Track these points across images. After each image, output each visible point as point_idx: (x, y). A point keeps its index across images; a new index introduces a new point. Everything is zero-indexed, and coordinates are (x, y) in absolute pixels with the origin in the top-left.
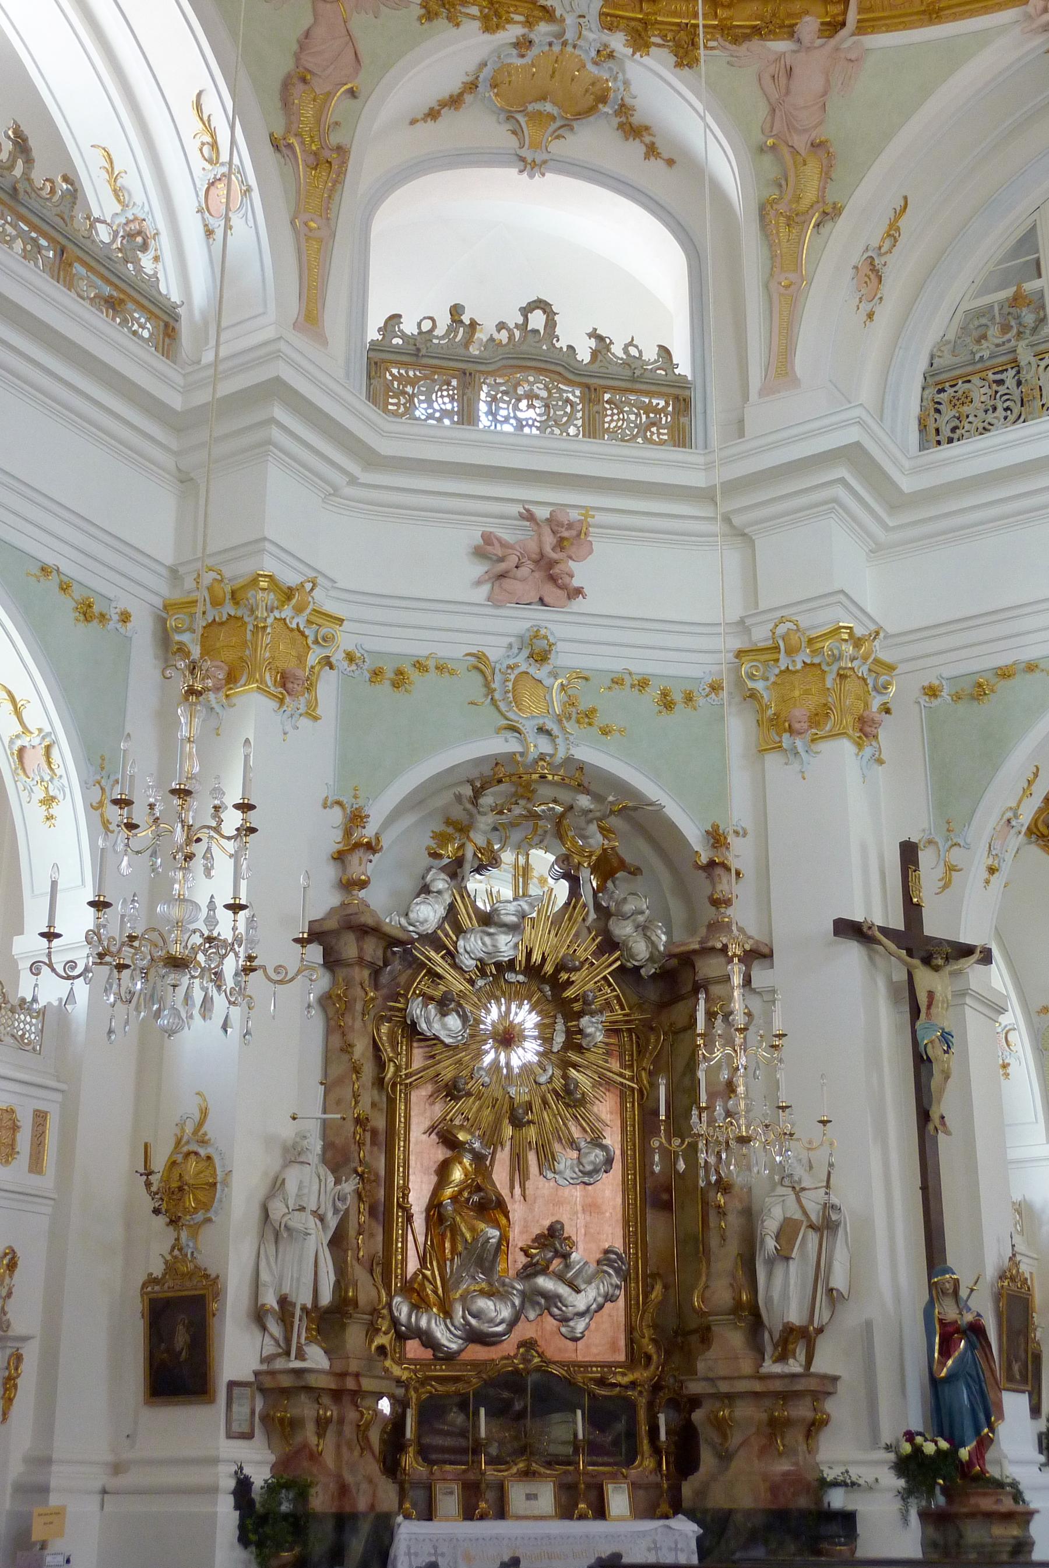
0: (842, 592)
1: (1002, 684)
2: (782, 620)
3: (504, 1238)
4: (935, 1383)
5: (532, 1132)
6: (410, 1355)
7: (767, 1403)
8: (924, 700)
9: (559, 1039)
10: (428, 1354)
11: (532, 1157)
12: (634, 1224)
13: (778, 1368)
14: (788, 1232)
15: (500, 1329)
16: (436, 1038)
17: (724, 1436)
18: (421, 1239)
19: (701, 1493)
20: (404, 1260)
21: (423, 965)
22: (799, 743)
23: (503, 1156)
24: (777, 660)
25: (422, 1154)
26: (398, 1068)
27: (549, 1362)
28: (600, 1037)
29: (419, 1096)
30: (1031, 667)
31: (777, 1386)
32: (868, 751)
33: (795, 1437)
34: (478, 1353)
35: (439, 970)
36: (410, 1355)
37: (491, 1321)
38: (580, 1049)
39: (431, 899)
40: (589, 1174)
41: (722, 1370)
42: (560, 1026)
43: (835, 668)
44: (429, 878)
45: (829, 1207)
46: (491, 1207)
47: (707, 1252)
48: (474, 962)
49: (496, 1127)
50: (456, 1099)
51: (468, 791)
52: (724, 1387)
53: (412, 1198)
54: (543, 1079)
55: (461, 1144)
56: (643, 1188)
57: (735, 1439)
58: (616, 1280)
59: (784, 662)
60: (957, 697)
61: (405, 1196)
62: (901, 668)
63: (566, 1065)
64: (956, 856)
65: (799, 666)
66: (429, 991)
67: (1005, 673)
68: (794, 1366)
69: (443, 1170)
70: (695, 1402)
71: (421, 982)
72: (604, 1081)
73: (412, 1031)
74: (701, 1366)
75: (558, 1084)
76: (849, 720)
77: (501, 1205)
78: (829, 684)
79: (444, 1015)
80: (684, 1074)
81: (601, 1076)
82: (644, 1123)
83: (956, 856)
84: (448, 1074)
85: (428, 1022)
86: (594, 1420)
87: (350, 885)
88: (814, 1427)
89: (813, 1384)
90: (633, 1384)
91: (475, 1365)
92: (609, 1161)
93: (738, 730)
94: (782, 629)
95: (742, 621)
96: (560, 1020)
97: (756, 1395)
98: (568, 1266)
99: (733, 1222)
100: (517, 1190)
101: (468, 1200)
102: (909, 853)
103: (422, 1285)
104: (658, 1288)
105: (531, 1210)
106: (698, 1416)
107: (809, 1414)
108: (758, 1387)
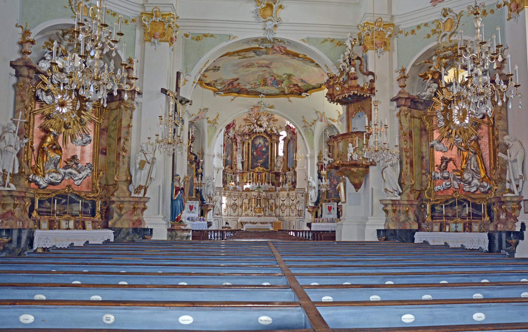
0: (172, 4)
1: (204, 38)
2: (156, 7)
3: (61, 158)
4: (172, 200)
5: (70, 131)
6: (32, 187)
7: (133, 203)
8: (184, 37)
9: (78, 107)
10: (37, 187)
11: (69, 137)
12: (94, 157)
13: (136, 195)
14: (142, 164)
15: (59, 181)
16: (44, 101)
17: (121, 211)
18: (36, 156)
19: (114, 224)
20: (31, 161)
21: (41, 80)
22: (156, 41)
23: (61, 136)
24: (152, 18)
25: (37, 132)
26: (32, 108)
27: (74, 191)
28: (91, 108)
29: (37, 117)
30: (212, 36)
31: (136, 200)
32: (172, 47)
33: (139, 211)
34: (52, 187)
35: (46, 83)
36: (32, 187)
37: (56, 179)
38: (85, 110)
39: (46, 61)
40: (85, 143)
41: (121, 195)
42: (79, 103)
43: (168, 24)
44: (45, 55)
45: (154, 158)
46: (58, 150)
47: (118, 166)
48: (57, 82)
49: (60, 128)
50: (49, 119)
51: (61, 32)
52: (122, 199)
53: (34, 145)
54: (73, 117)
55: (51, 132)
56: (99, 149)
57: (123, 212)
58: (89, 171)
59: (154, 19)
60: (193, 38)
61: (32, 144)
62: (180, 28)
63: (79, 114)
64: (187, 78)
65: (158, 21)
66: (42, 88)
67: (205, 36)
68: (141, 195)
69: (43, 139)
70: (113, 202)
71: (40, 85)
72: (91, 121)
73: (37, 99)
74: (115, 194)
75: (78, 119)
76: (169, 38)
77: (60, 149)
78: (166, 27)
79: (47, 95)
80: (113, 121)
81: (90, 118)
82: (102, 131)
83: (187, 78)
84: (47, 112)
85: (42, 97)
86: (85, 205)
87: (24, 53)
88: (144, 209)
89: (146, 200)
90: (94, 197)
91: (50, 190)
92: (90, 141)
93: (139, 33)
94: (155, 10)
95: (143, 5)
96: (79, 102)
97: (130, 201)
98: (77, 167)
99: (126, 159)
100: (64, 146)
101: (52, 147)
102: (178, 74)
103: (37, 169)
104: (101, 173)
105: (68, 151)
106: (114, 206)
107: (143, 206)
108: (132, 200)
